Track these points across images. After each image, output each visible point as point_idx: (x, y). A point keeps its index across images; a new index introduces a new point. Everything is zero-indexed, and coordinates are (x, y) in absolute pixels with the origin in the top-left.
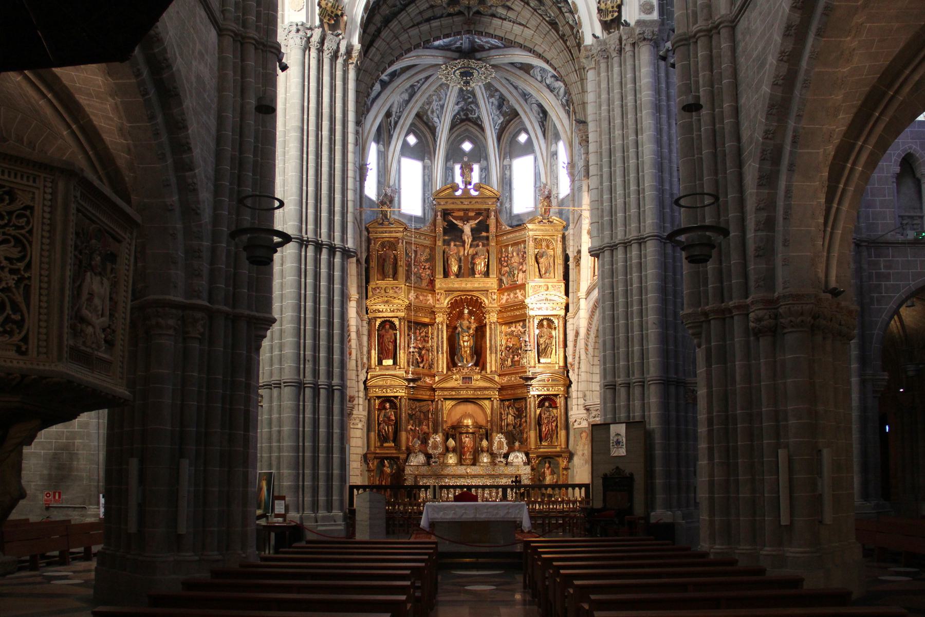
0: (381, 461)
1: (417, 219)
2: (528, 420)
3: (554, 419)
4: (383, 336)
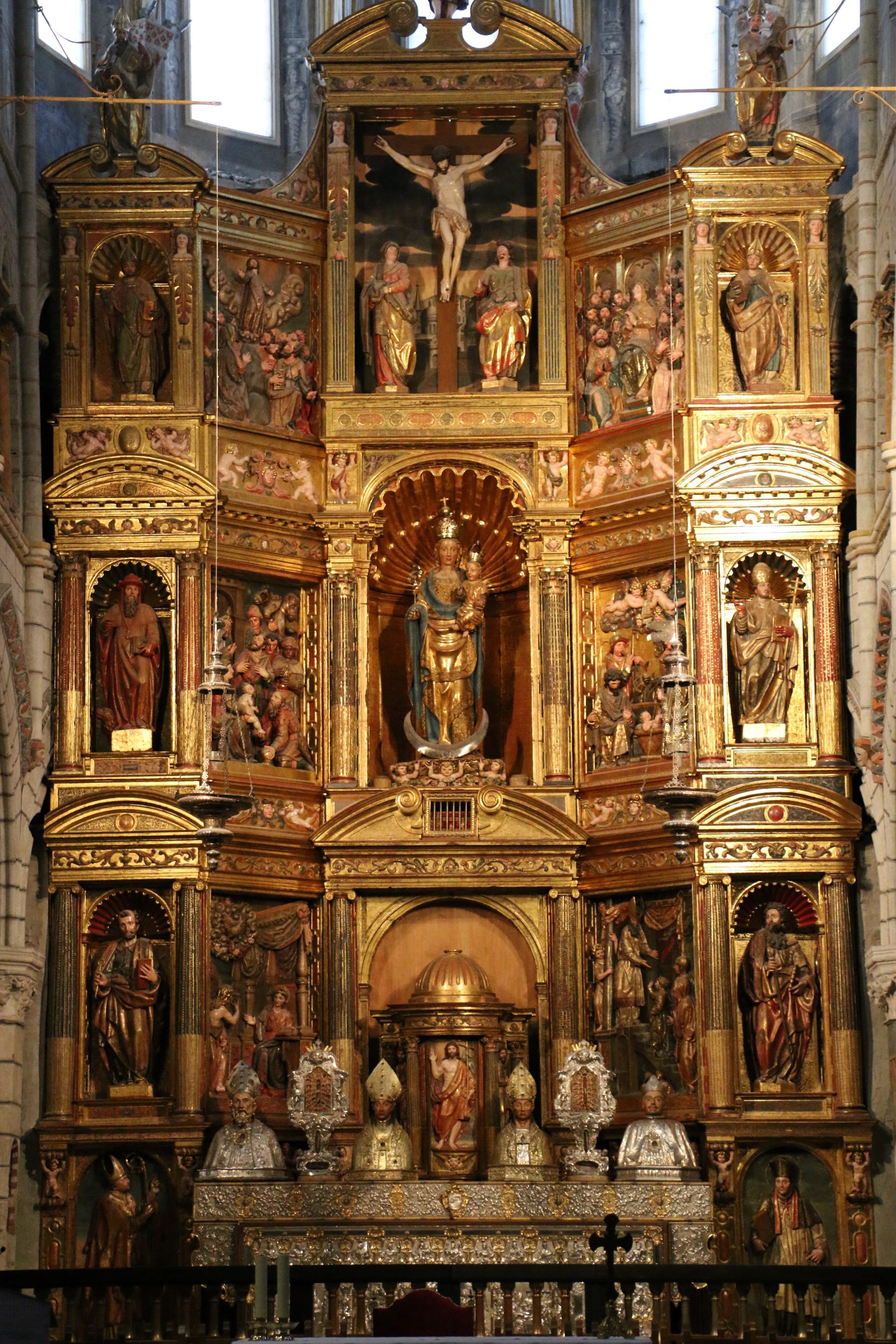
0: (97, 1163)
2: (699, 983)
3: (805, 979)
4: (115, 630)
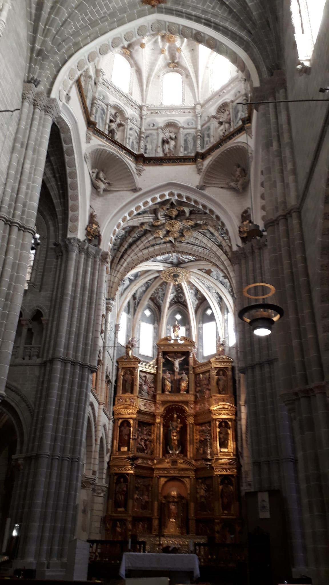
1: (146, 357)
